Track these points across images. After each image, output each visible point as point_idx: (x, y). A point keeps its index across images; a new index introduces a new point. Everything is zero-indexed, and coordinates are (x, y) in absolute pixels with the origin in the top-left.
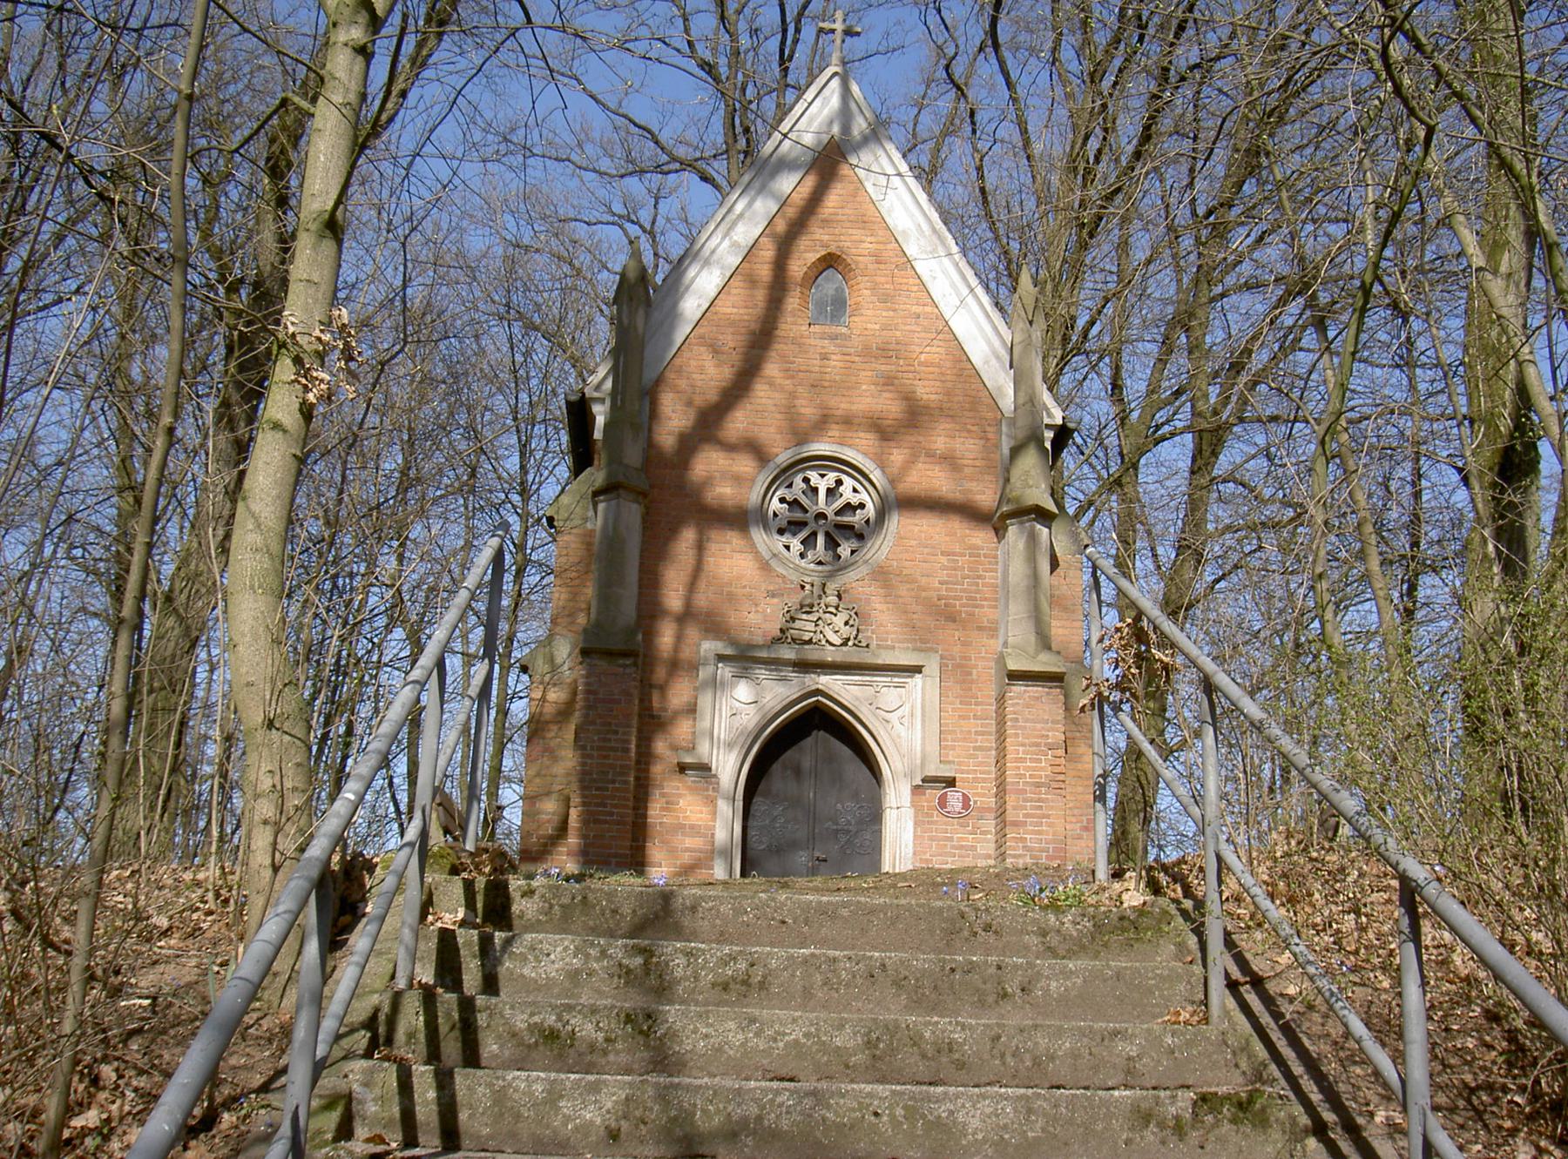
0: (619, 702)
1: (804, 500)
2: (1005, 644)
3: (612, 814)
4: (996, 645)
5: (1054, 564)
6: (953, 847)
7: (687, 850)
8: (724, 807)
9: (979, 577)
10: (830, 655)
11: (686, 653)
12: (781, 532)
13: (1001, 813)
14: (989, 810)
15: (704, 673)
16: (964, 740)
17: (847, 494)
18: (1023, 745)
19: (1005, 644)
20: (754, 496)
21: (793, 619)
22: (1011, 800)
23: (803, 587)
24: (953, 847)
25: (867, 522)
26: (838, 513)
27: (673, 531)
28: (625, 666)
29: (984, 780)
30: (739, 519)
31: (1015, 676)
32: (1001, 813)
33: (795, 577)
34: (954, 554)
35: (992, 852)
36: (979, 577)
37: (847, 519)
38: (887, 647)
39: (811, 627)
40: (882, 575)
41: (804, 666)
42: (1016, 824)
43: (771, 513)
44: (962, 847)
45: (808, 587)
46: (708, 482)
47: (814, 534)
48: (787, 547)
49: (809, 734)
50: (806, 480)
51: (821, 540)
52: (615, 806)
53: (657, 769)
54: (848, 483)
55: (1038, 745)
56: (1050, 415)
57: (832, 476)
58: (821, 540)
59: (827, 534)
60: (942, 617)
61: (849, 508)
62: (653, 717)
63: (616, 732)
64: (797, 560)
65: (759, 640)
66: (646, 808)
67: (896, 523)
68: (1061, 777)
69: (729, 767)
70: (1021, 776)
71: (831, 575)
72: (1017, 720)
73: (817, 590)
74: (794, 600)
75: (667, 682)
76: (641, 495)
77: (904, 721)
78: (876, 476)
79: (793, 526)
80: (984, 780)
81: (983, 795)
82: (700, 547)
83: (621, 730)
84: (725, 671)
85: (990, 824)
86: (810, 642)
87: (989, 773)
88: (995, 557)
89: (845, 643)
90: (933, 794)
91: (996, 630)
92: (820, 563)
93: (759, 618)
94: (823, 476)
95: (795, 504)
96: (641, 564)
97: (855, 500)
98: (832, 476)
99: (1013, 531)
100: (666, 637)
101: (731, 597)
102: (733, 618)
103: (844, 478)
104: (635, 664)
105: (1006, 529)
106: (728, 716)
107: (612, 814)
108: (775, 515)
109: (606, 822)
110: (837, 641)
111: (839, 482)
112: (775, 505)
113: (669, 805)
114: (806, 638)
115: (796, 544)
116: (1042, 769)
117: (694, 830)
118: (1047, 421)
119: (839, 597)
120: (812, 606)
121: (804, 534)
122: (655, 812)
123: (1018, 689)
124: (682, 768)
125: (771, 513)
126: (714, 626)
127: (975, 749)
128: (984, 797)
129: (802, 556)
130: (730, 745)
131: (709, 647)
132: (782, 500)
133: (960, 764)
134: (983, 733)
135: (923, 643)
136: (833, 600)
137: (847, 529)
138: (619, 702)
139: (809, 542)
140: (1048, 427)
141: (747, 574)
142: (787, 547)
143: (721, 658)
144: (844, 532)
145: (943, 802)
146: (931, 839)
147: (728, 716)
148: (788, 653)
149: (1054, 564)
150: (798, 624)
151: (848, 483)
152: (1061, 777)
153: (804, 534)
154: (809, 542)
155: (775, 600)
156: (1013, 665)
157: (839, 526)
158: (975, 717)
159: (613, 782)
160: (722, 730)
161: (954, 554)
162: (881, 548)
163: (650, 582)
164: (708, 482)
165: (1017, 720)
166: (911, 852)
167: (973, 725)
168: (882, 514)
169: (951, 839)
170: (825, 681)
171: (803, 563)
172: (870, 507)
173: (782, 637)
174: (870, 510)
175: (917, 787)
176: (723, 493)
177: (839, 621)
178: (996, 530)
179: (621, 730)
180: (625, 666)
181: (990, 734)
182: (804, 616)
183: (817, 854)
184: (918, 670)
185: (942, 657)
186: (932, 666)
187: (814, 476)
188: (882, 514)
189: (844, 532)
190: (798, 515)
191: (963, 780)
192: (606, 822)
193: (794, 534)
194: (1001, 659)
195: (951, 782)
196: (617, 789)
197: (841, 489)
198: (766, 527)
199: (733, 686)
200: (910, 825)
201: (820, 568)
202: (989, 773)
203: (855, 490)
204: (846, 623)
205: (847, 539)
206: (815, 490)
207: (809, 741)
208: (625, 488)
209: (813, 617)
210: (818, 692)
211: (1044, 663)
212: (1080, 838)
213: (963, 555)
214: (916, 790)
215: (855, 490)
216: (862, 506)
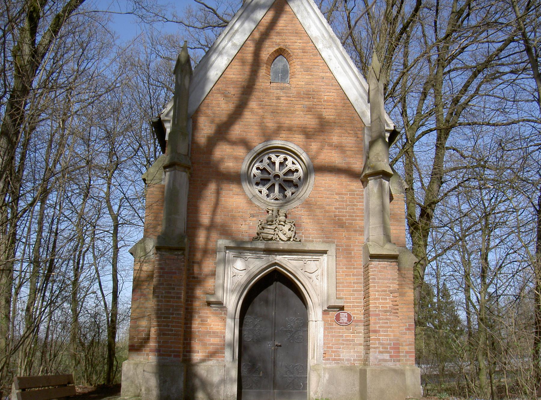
0: (175, 273)
1: (268, 169)
2: (368, 239)
3: (172, 330)
4: (364, 238)
5: (391, 198)
6: (343, 340)
7: (212, 344)
8: (230, 322)
9: (354, 205)
10: (282, 246)
11: (211, 246)
12: (257, 184)
13: (367, 325)
14: (360, 321)
15: (219, 256)
16: (348, 286)
17: (289, 164)
18: (378, 291)
19: (368, 239)
20: (244, 167)
21: (263, 228)
22: (372, 319)
23: (268, 212)
24: (343, 340)
25: (300, 178)
26: (285, 174)
27: (205, 185)
28: (178, 255)
29: (358, 306)
30: (237, 178)
31: (373, 257)
32: (367, 325)
33: (264, 207)
34: (342, 194)
35: (362, 342)
36: (354, 205)
37: (289, 177)
38: (310, 241)
39: (272, 232)
40: (308, 205)
41: (269, 251)
42: (375, 331)
43: (252, 175)
44: (347, 340)
45: (270, 212)
46: (222, 160)
47: (273, 185)
48: (261, 192)
49: (272, 284)
50: (270, 159)
51: (277, 188)
52: (172, 326)
53: (197, 304)
54: (290, 159)
55: (385, 291)
56: (388, 125)
57: (282, 156)
58: (277, 188)
59: (280, 185)
60: (338, 225)
61: (291, 172)
62: (194, 278)
63: (174, 289)
64: (265, 198)
65: (246, 238)
66: (191, 324)
67: (313, 179)
68: (396, 307)
69: (232, 302)
70: (377, 307)
71: (282, 206)
72: (374, 279)
73: (275, 213)
74: (264, 218)
75: (201, 260)
76: (186, 168)
77: (318, 278)
78: (304, 156)
79: (263, 181)
80: (358, 306)
81: (358, 314)
82: (218, 193)
83: (176, 288)
84: (230, 254)
85: (361, 328)
86: (271, 239)
87: (360, 302)
88: (362, 195)
90: (333, 314)
91: (363, 231)
92: (277, 199)
93: (247, 228)
94: (277, 156)
95: (264, 170)
96: (188, 202)
97: (293, 168)
98: (282, 156)
99: (372, 183)
100: (201, 238)
101: (233, 218)
102: (234, 227)
103: (288, 157)
104: (183, 254)
105: (367, 182)
106: (231, 277)
107: (172, 330)
108: (254, 176)
109: (169, 335)
110: (286, 239)
111: (286, 159)
112: (254, 171)
113: (203, 321)
114: (270, 237)
115: (265, 190)
116: (387, 303)
117: (215, 334)
118: (386, 128)
119: (286, 216)
120: (272, 221)
121: (268, 186)
122: (196, 325)
123: (375, 263)
124: (209, 304)
125: (252, 175)
126: (225, 232)
127: (353, 291)
128: (358, 314)
129: (268, 196)
130: (233, 291)
131: (222, 242)
132: (258, 169)
133: (346, 298)
134: (357, 283)
135: (328, 238)
136: (282, 218)
137: (290, 183)
138: (175, 273)
139: (271, 189)
140: (387, 131)
141: (241, 205)
142: (261, 192)
143: (228, 248)
144: (288, 184)
145: (338, 318)
146: (332, 336)
147: (231, 277)
148: (261, 245)
149: (391, 198)
150: (266, 231)
151: (290, 159)
152: (396, 307)
153: (268, 186)
154: (271, 189)
155: (255, 218)
156: (372, 252)
157: (285, 181)
158: (354, 275)
159: (173, 314)
160: (228, 284)
161: (342, 194)
162: (307, 191)
163: (193, 210)
164: (222, 160)
165: (374, 279)
166: (322, 342)
167: (353, 279)
168: (307, 175)
169: (342, 336)
170: (279, 258)
171: (268, 199)
172: (301, 171)
173: (258, 237)
174: (301, 173)
175: (325, 311)
176: (229, 165)
177: (286, 228)
178: (363, 182)
179: (176, 288)
180: (178, 255)
181: (360, 283)
182: (269, 227)
183: (277, 343)
184: (325, 252)
185: (337, 246)
186: (332, 250)
187: (273, 157)
188: (307, 175)
189: (288, 184)
190: (266, 176)
191: (348, 307)
192: (169, 335)
193: (264, 185)
194: (366, 247)
195: (342, 308)
196: (174, 318)
197: (287, 163)
198: (250, 182)
199: (234, 262)
200: (322, 330)
201: (277, 202)
202: (360, 302)
203: (293, 163)
204: (289, 230)
205: (290, 187)
206: (274, 163)
207: (272, 287)
208: (179, 165)
209: (273, 227)
210: (276, 264)
211: (388, 250)
212: (405, 334)
213: (346, 194)
214: (325, 312)
215: (293, 163)
216: (297, 171)
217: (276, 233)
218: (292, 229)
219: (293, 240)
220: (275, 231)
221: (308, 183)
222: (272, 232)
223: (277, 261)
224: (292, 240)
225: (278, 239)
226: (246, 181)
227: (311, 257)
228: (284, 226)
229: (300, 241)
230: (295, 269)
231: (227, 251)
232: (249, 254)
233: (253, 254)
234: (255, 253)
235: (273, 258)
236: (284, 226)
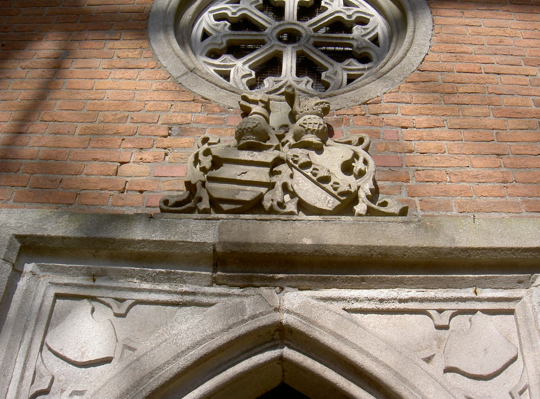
10: (307, 233)
12: (214, 54)
21: (217, 162)
39: (261, 174)
41: (250, 266)
51: (289, 63)
58: (289, 63)
65: (131, 204)
86: (256, 206)
89: (347, 203)
101: (97, 135)
102: (93, 172)
108: (205, 35)
148: (201, 232)
170: (295, 303)
182: (245, 155)
199: (51, 320)
204: (347, 168)
210: (282, 334)
217: (279, 180)
218: (358, 165)
219: (370, 212)
220: (272, 173)
221: (407, 39)
222: (261, 174)
223: (286, 318)
224: (360, 208)
225: (291, 207)
226: (166, 31)
227: (469, 293)
228: (319, 150)
229: (404, 212)
230: (389, 358)
231: (29, 267)
232: (136, 283)
233: (154, 279)
234: (169, 278)
235: (264, 299)
236: (319, 150)
